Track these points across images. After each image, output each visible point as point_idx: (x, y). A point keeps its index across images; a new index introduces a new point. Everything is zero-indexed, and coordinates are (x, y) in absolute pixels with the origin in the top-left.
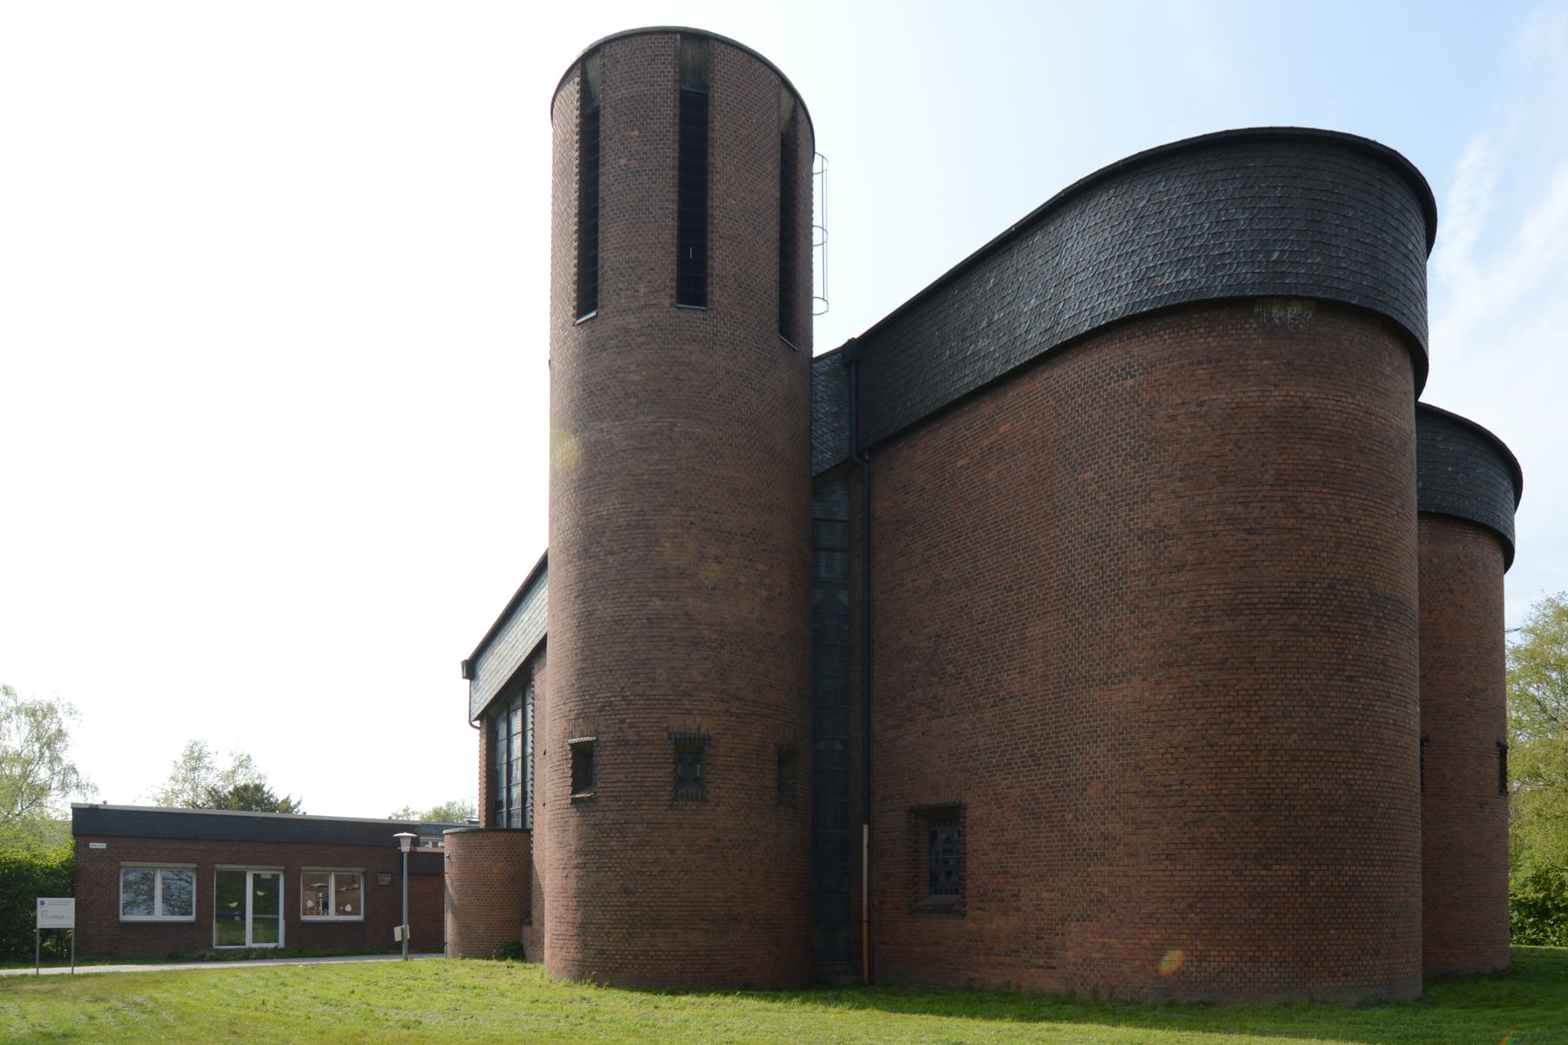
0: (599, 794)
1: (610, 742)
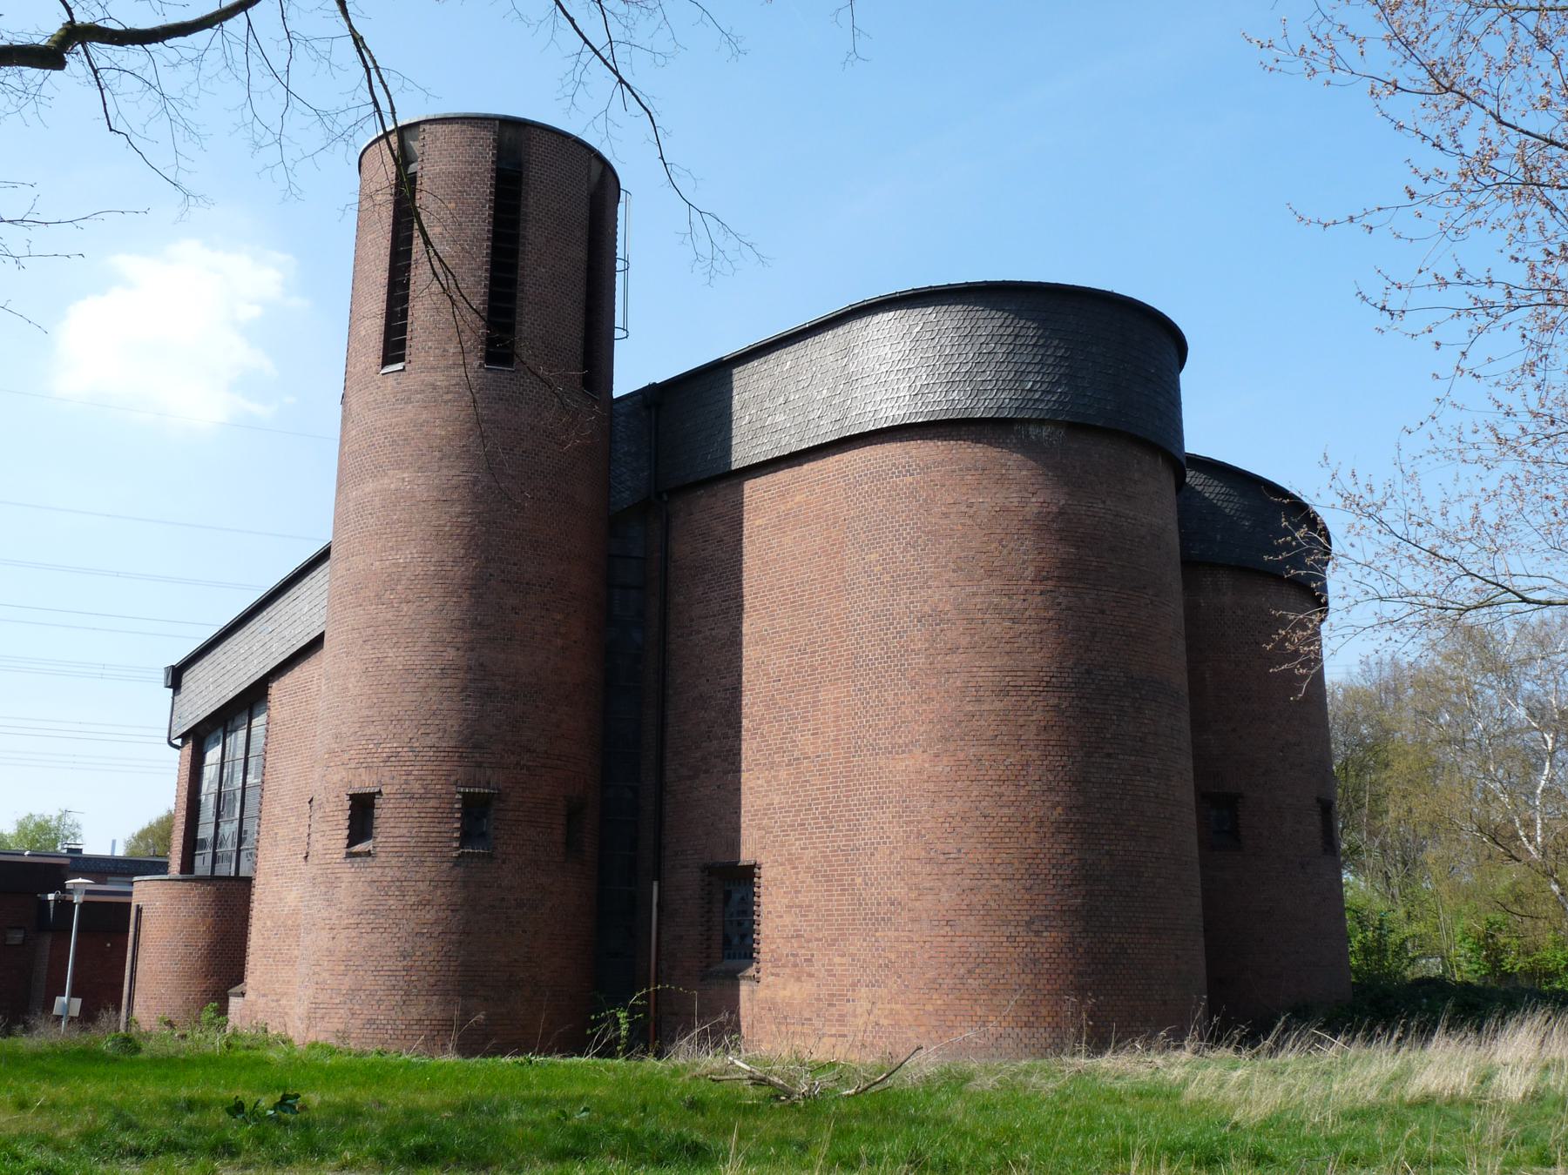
0: (378, 849)
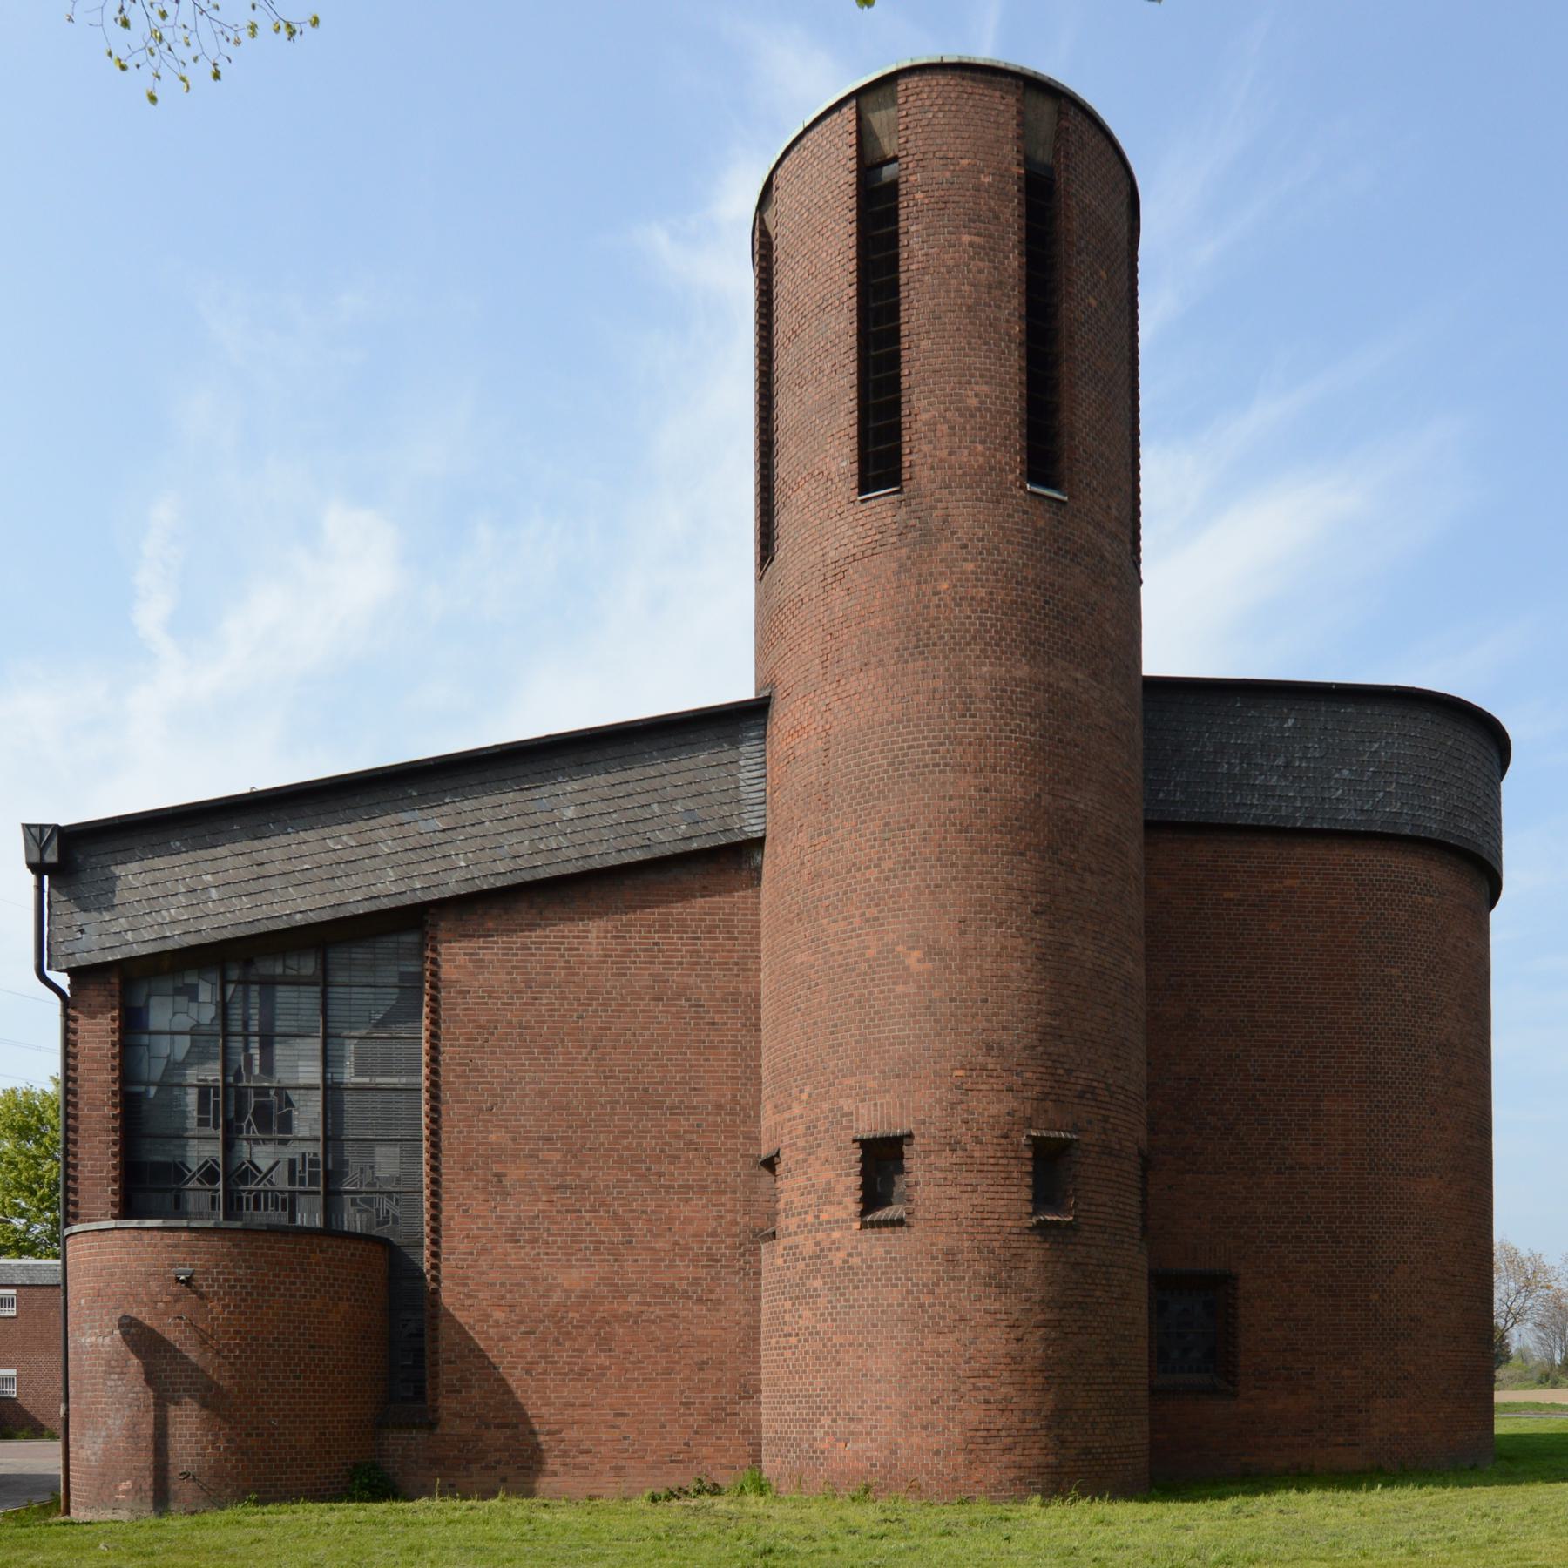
0: (1080, 1220)
1: (1094, 1145)
